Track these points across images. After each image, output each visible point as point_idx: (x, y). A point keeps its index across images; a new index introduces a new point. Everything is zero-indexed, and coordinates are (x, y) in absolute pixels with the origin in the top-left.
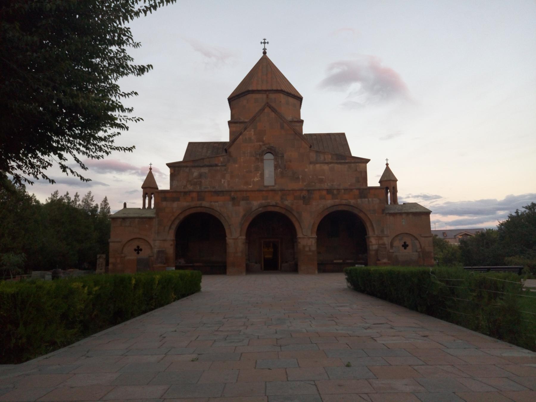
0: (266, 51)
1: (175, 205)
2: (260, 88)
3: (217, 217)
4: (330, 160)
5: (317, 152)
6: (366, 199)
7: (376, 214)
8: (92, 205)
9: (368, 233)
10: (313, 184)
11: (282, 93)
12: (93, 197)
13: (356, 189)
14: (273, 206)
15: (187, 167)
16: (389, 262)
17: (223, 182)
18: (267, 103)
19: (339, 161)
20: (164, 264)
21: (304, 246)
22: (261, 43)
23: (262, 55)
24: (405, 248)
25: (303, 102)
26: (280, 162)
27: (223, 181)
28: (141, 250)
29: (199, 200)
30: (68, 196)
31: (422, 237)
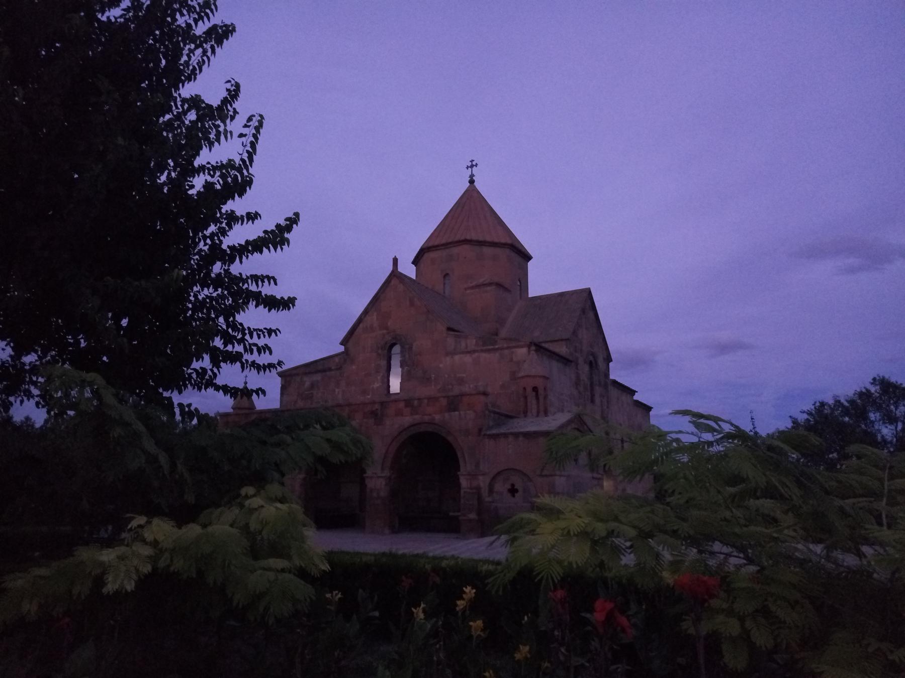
0: (474, 178)
2: (436, 243)
6: (457, 413)
10: (450, 387)
13: (444, 397)
15: (298, 375)
17: (337, 393)
19: (485, 348)
23: (469, 184)
24: (514, 496)
26: (407, 356)
27: (337, 390)
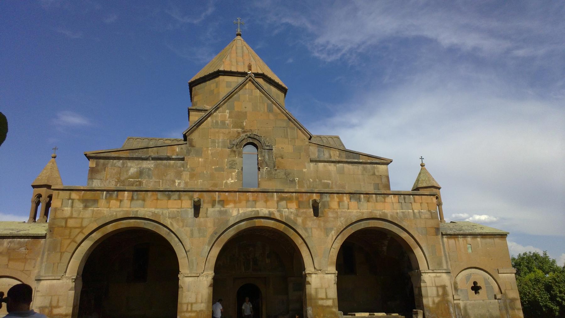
2: (234, 69)
3: (164, 236)
4: (337, 159)
15: (119, 158)
21: (316, 289)
27: (177, 181)
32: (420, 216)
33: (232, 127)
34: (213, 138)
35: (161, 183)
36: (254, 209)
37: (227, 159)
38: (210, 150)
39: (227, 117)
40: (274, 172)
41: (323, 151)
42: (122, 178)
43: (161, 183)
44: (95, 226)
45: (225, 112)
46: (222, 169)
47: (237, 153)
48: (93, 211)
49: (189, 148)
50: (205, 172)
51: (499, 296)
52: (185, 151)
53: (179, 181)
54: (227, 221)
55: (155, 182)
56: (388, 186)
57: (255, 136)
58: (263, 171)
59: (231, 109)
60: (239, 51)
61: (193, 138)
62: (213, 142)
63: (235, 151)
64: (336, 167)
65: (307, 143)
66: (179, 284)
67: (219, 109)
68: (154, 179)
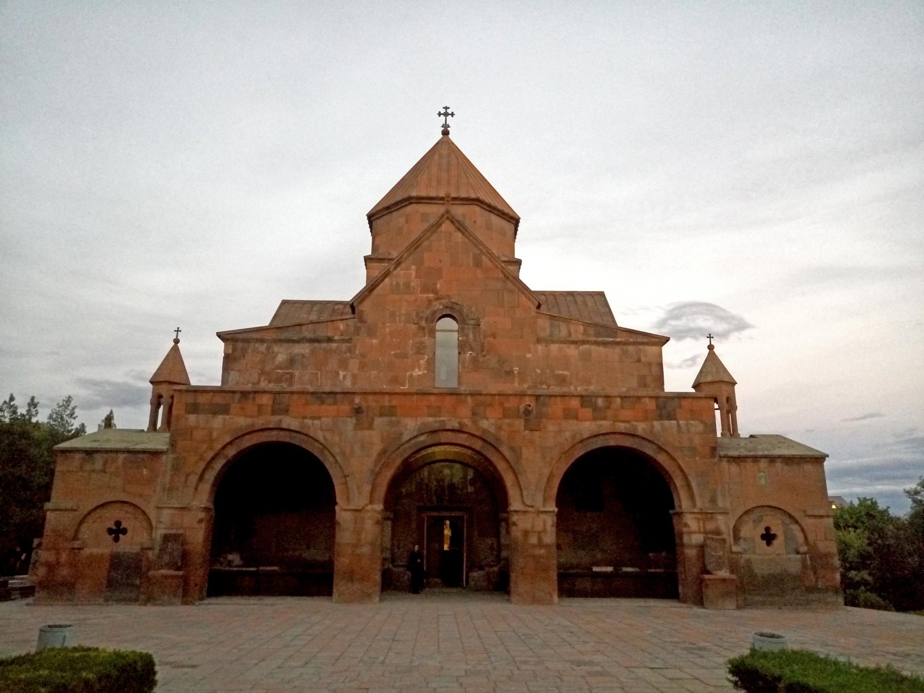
1: (218, 422)
4: (581, 337)
5: (552, 317)
6: (674, 422)
7: (697, 458)
8: (72, 425)
9: (676, 504)
11: (478, 205)
12: (74, 408)
13: (652, 397)
14: (452, 431)
15: (262, 341)
16: (734, 577)
18: (448, 212)
20: (178, 569)
21: (526, 533)
22: (440, 114)
23: (442, 136)
24: (769, 544)
25: (519, 228)
26: (471, 336)
27: (342, 373)
28: (124, 531)
29: (274, 413)
30: (12, 403)
31: (808, 516)
32: (688, 430)
33: (420, 292)
34: (392, 310)
35: (319, 375)
36: (438, 419)
37: (413, 340)
38: (388, 327)
39: (413, 276)
40: (481, 359)
41: (559, 326)
42: (267, 369)
43: (319, 375)
44: (228, 439)
45: (408, 268)
46: (405, 356)
47: (426, 331)
48: (225, 420)
49: (359, 324)
50: (381, 359)
51: (804, 549)
52: (353, 329)
53: (344, 373)
54: (401, 434)
55: (312, 373)
56: (660, 379)
57: (455, 305)
58: (465, 357)
59: (419, 263)
60: (445, 161)
61: (364, 310)
62: (393, 315)
63: (423, 328)
64: (577, 351)
65: (533, 314)
66: (336, 519)
67: (401, 265)
68: (310, 370)
